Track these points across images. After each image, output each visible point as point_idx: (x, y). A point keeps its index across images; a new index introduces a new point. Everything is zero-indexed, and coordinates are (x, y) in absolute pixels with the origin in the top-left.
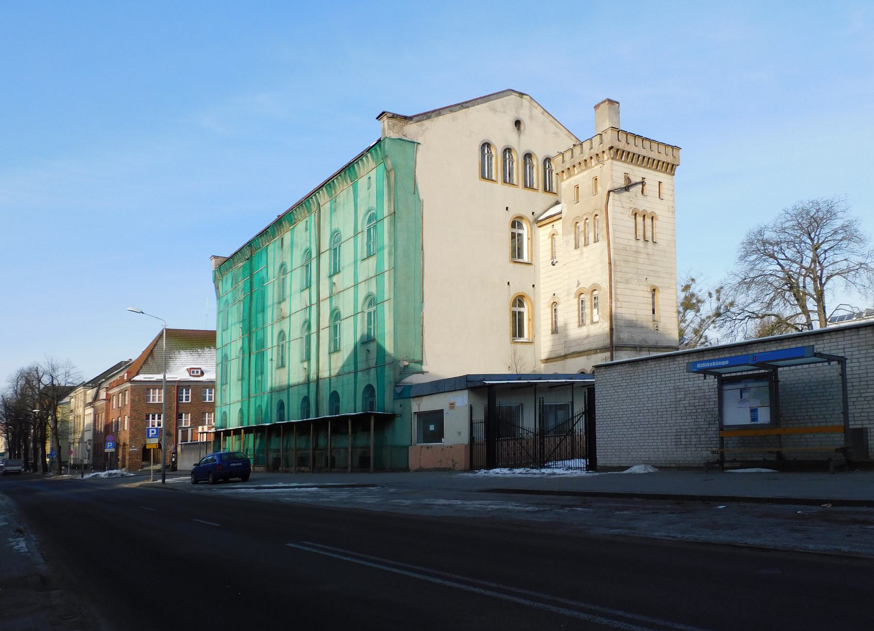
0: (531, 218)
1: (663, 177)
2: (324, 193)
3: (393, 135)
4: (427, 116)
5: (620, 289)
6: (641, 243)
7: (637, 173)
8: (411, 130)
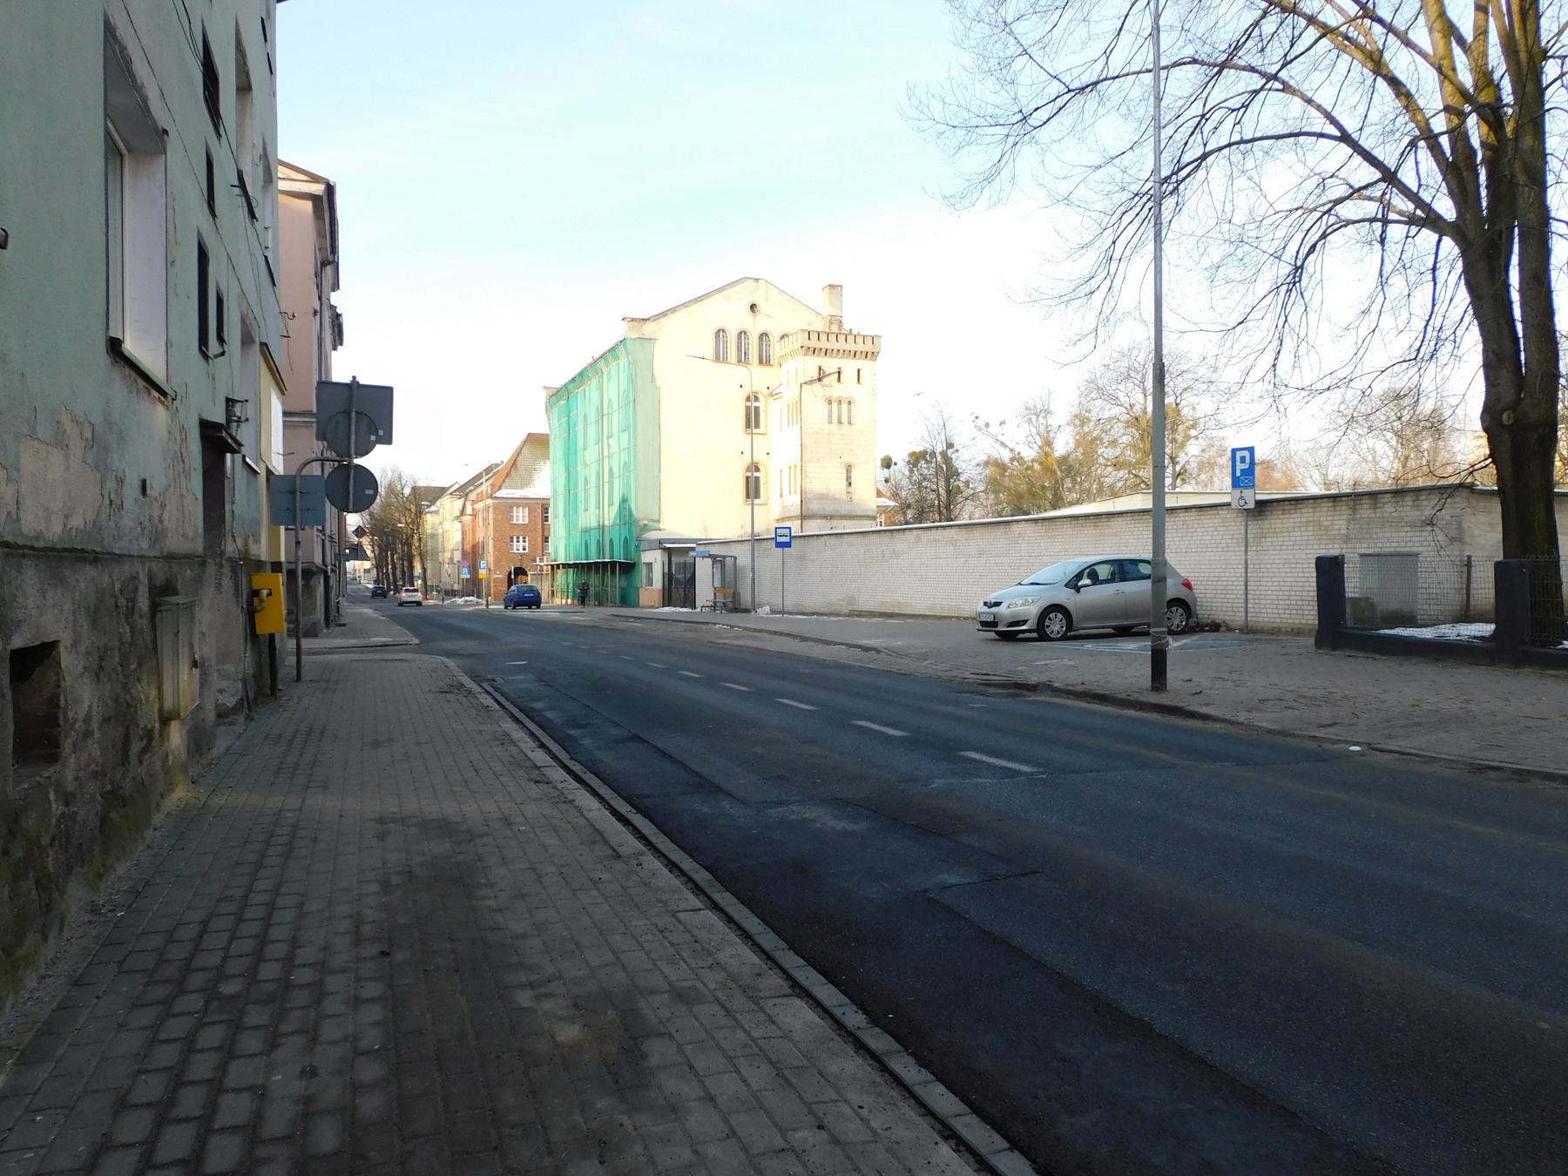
0: (766, 392)
1: (864, 364)
2: (602, 362)
3: (632, 335)
4: (664, 314)
5: (810, 468)
6: (835, 426)
7: (830, 364)
8: (649, 328)
